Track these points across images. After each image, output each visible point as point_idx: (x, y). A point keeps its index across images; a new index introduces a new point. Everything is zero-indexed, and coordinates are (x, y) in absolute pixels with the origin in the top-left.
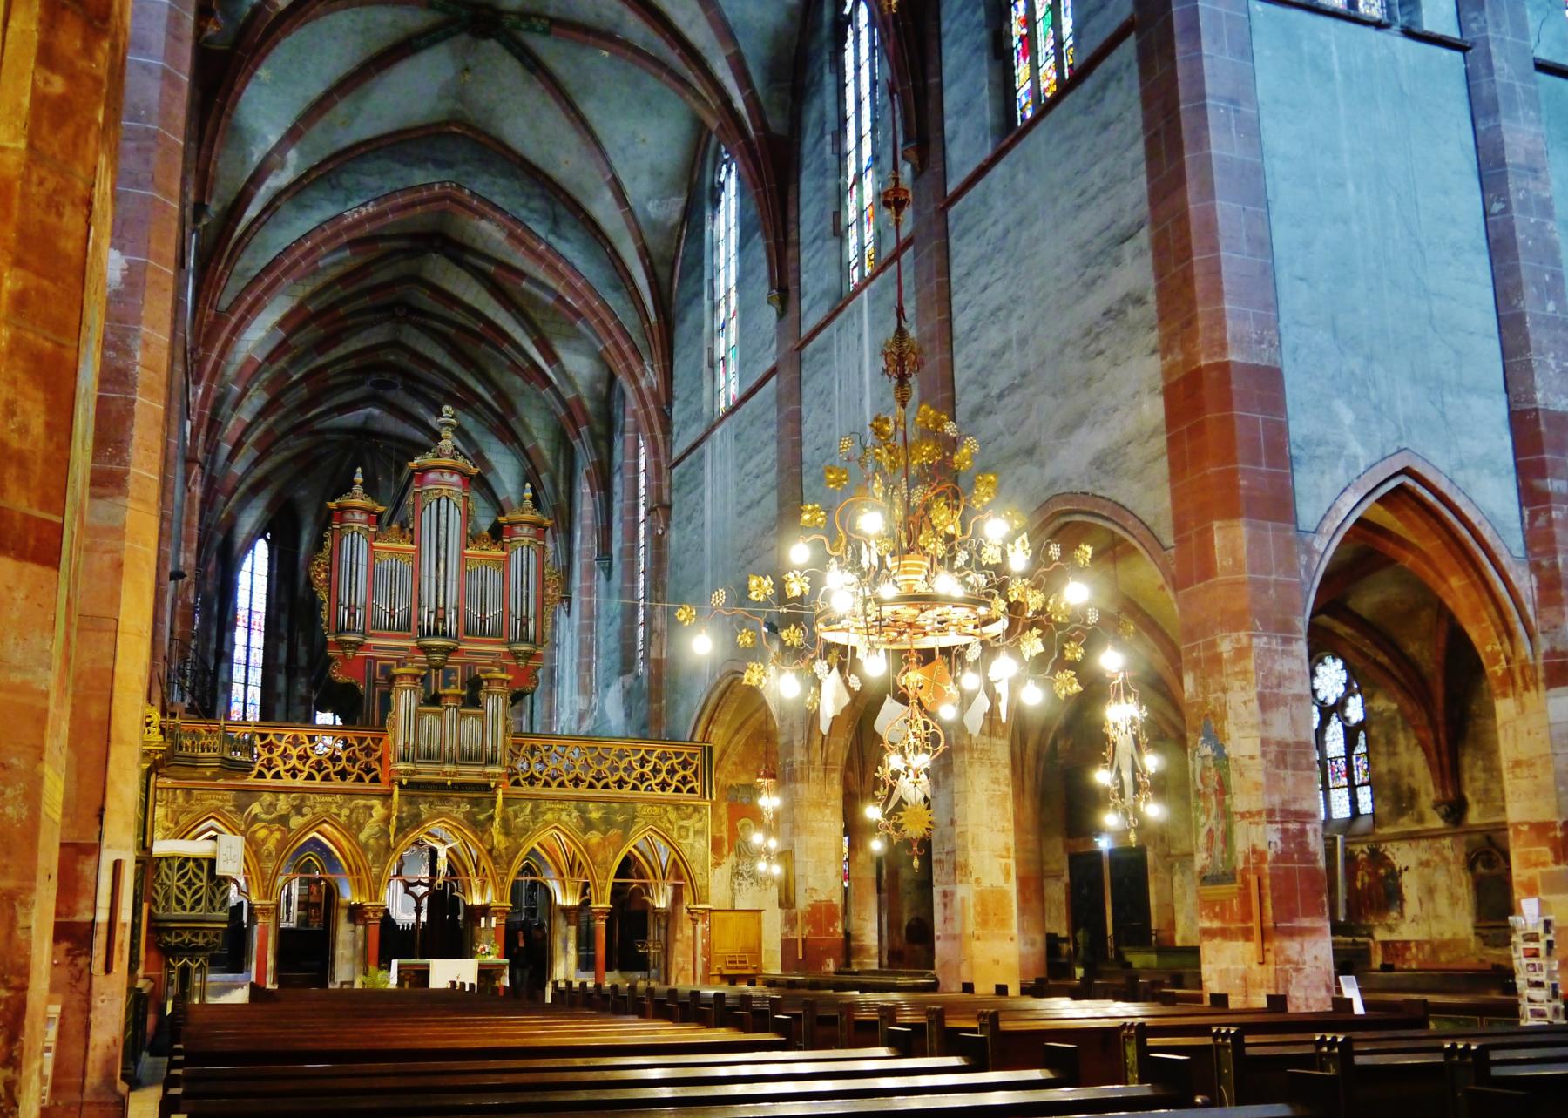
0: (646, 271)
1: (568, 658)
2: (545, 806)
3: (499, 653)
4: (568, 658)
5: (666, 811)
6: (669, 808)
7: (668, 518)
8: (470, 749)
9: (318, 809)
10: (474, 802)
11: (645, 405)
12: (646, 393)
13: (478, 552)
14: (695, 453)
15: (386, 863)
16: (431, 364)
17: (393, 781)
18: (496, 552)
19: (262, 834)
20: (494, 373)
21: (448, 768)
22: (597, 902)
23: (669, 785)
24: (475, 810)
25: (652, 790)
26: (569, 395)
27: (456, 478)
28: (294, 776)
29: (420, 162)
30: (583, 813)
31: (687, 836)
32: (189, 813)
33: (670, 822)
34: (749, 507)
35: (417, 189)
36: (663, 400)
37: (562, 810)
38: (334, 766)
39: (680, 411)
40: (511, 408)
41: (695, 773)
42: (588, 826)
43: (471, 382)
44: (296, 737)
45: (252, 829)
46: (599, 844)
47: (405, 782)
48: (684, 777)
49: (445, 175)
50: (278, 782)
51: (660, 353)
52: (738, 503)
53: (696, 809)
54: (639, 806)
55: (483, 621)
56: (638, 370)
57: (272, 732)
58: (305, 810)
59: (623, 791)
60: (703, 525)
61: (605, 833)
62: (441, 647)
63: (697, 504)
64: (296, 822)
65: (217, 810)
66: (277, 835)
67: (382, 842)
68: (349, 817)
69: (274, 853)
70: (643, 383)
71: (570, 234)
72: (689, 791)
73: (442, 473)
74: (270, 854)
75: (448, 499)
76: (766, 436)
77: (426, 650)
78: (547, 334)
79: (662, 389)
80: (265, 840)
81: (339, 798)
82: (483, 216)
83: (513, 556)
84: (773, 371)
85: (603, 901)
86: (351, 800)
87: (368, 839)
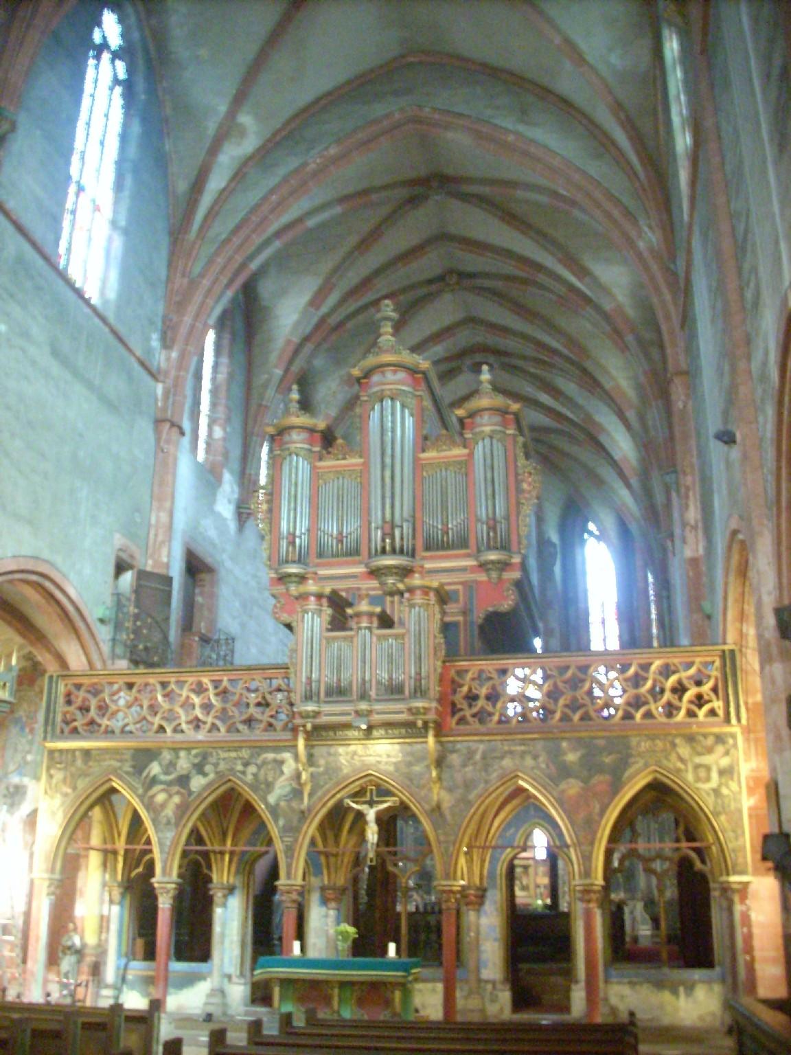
3: (463, 569)
5: (674, 745)
6: (678, 741)
12: (646, 254)
16: (505, 330)
18: (459, 452)
19: (161, 798)
20: (562, 322)
21: (363, 706)
26: (608, 306)
27: (402, 375)
28: (197, 727)
31: (708, 779)
32: (86, 775)
38: (241, 713)
40: (582, 350)
41: (715, 690)
44: (200, 684)
45: (151, 793)
50: (179, 737)
53: (720, 739)
56: (633, 234)
57: (173, 680)
58: (208, 768)
61: (585, 781)
62: (387, 567)
64: (197, 783)
66: (177, 799)
68: (255, 775)
69: (173, 821)
70: (641, 245)
74: (168, 823)
77: (375, 573)
80: (163, 805)
81: (245, 753)
82: (447, 127)
86: (259, 755)
87: (279, 799)
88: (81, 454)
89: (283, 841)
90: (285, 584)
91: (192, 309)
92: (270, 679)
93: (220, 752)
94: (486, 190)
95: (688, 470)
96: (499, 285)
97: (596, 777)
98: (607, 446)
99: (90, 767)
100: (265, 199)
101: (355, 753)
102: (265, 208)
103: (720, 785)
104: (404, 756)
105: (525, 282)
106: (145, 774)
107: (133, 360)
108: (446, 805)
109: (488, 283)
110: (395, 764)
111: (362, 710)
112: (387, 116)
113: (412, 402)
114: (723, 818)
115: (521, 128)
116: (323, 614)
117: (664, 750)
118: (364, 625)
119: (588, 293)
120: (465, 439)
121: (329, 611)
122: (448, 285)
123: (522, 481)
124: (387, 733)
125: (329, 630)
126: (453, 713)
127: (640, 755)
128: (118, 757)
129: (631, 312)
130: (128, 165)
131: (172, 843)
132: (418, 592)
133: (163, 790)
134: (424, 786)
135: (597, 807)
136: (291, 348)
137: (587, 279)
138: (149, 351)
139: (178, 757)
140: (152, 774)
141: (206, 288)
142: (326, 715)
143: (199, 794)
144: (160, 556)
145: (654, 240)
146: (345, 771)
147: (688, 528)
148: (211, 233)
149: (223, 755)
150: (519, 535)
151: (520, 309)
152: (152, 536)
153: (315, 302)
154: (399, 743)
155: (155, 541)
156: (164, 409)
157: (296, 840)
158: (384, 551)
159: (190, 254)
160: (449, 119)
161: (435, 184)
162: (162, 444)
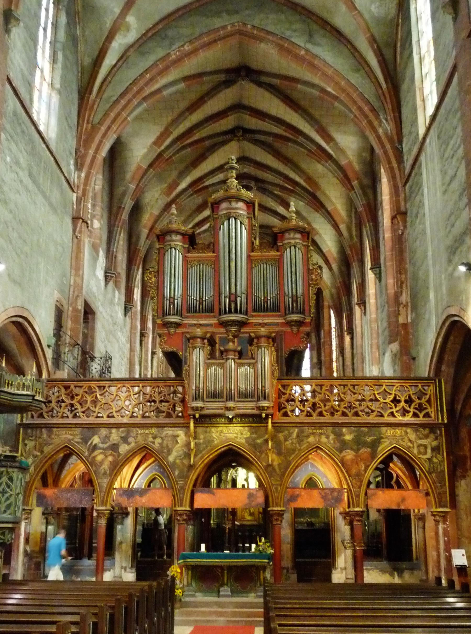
0: (374, 52)
1: (366, 343)
2: (308, 430)
3: (277, 324)
4: (366, 343)
5: (406, 432)
7: (405, 221)
8: (246, 389)
9: (139, 438)
10: (253, 430)
11: (383, 146)
13: (260, 254)
14: (416, 167)
15: (188, 478)
17: (190, 415)
18: (273, 253)
20: (304, 165)
21: (231, 404)
22: (354, 507)
23: (408, 412)
24: (254, 436)
25: (394, 416)
26: (343, 162)
29: (218, 14)
30: (339, 435)
31: (426, 453)
33: (410, 441)
34: (449, 184)
35: (218, 30)
36: (396, 138)
37: (321, 434)
39: (406, 144)
41: (429, 401)
42: (343, 445)
43: (292, 175)
45: (93, 455)
46: (352, 460)
47: (197, 416)
48: (420, 405)
49: (235, 19)
51: (390, 107)
52: (443, 184)
54: (384, 429)
55: (266, 301)
56: (376, 123)
57: (107, 385)
58: (131, 440)
59: (370, 417)
60: (424, 215)
61: (357, 451)
62: (233, 321)
63: (420, 202)
65: (69, 441)
66: (110, 459)
67: (186, 462)
68: (161, 444)
69: (108, 472)
70: (380, 131)
71: (323, 41)
72: (424, 416)
73: (230, 202)
74: (105, 473)
75: (235, 219)
76: (455, 121)
77: (224, 324)
78: (324, 125)
79: (394, 132)
80: (102, 463)
81: (154, 430)
82: (261, 40)
83: (285, 254)
84: (455, 68)
85: (358, 506)
86: (163, 432)
87: (175, 459)
88: (41, 240)
89: (177, 484)
90: (167, 328)
91: (94, 146)
92: (170, 386)
93: (138, 429)
94: (276, 82)
95: (403, 272)
96: (270, 139)
97: (363, 450)
98: (320, 244)
99: (53, 439)
100: (142, 75)
101: (222, 432)
102: (142, 83)
103: (432, 457)
104: (251, 434)
105: (288, 140)
106: (89, 443)
107: (63, 177)
108: (276, 463)
109: (262, 137)
110: (246, 438)
111: (230, 407)
112: (224, 27)
113: (246, 221)
114: (434, 475)
115: (309, 46)
116: (205, 349)
117: (401, 436)
118: (231, 357)
119: (332, 153)
120: (278, 246)
121: (209, 348)
122: (237, 136)
123: (312, 274)
124: (241, 420)
125: (209, 359)
126: (279, 412)
127: (386, 438)
128: (71, 432)
129: (357, 167)
130: (59, 45)
131: (107, 485)
132: (263, 339)
133: (101, 453)
134: (263, 452)
135: (363, 468)
136: (141, 173)
137: (332, 144)
138: (69, 173)
139: (111, 433)
140: (94, 444)
141: (104, 131)
142: (207, 409)
143: (126, 455)
144: (76, 304)
145: (389, 129)
146: (216, 442)
147: (402, 306)
148: (105, 95)
149: (140, 431)
150: (310, 306)
151: (278, 155)
152: (71, 293)
153: (157, 142)
154: (247, 427)
155: (73, 295)
156: (78, 210)
157: (186, 483)
158: (230, 312)
159: (93, 107)
160: (263, 35)
161: (243, 73)
162: (76, 234)
